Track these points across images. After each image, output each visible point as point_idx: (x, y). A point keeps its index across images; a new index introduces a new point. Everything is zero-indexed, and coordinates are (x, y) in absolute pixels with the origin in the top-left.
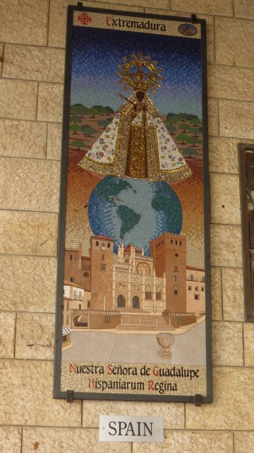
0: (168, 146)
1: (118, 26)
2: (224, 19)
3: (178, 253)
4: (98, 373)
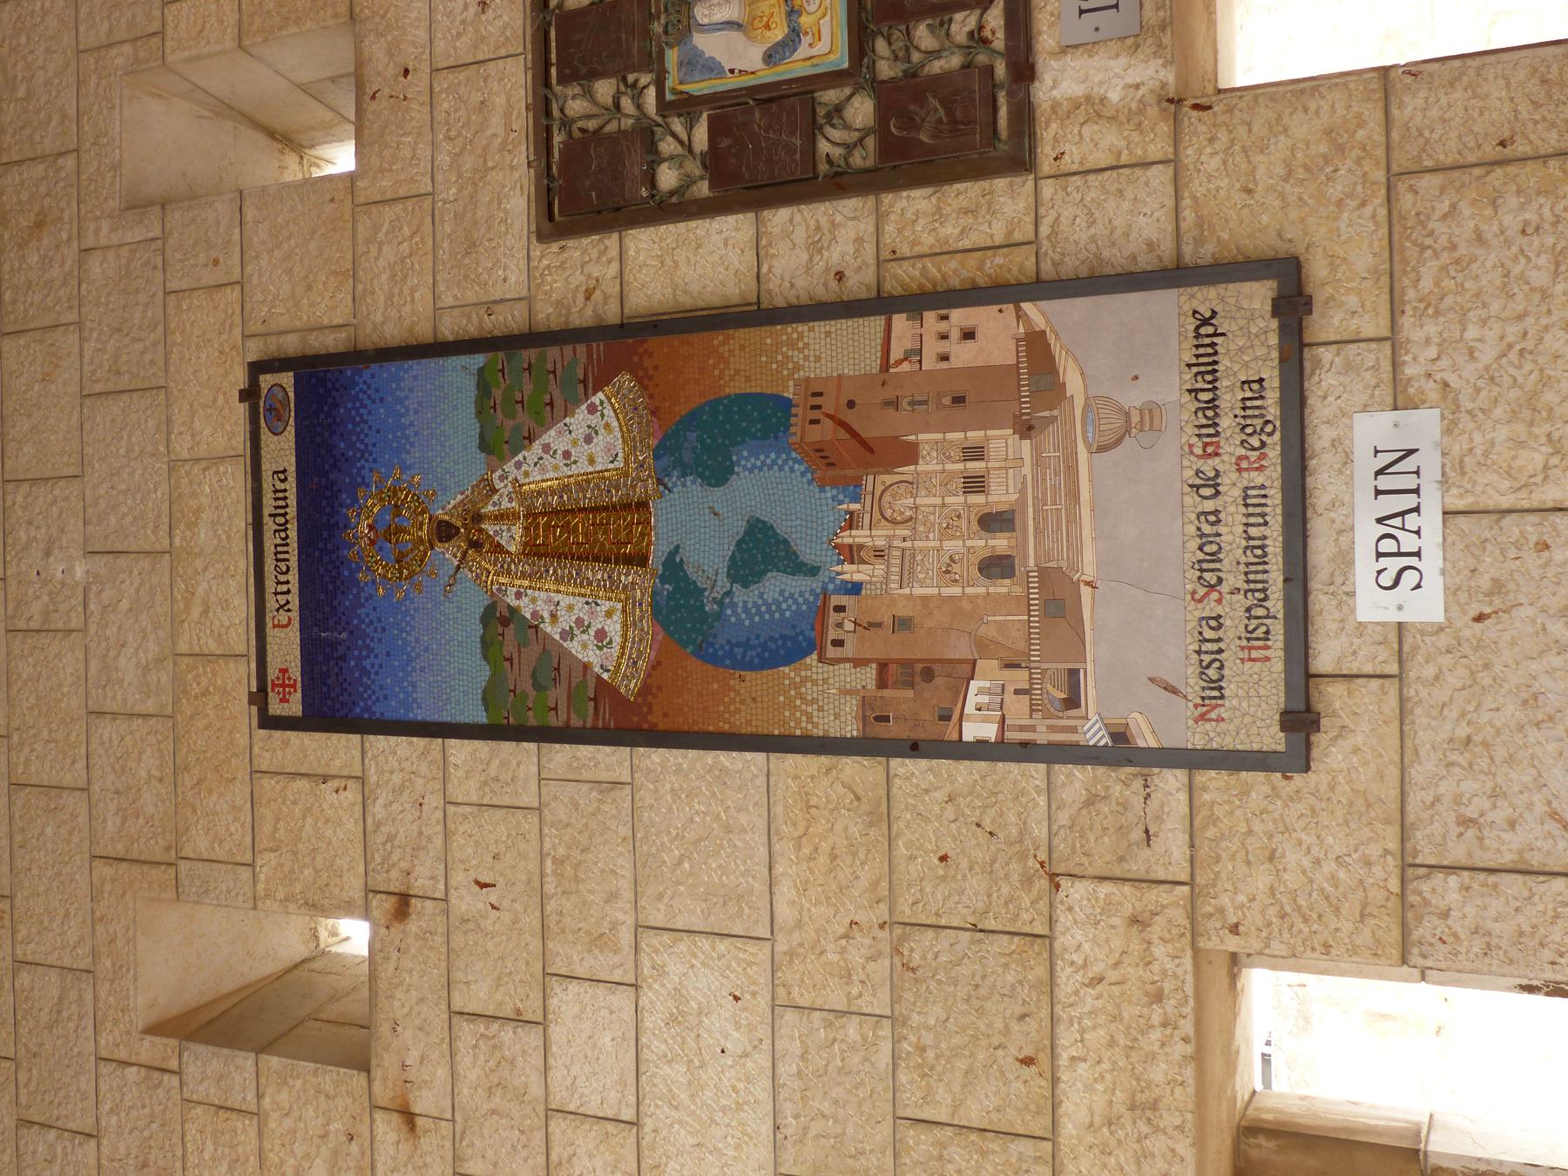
0: (560, 445)
1: (290, 597)
2: (248, 307)
3: (844, 402)
4: (1221, 633)
